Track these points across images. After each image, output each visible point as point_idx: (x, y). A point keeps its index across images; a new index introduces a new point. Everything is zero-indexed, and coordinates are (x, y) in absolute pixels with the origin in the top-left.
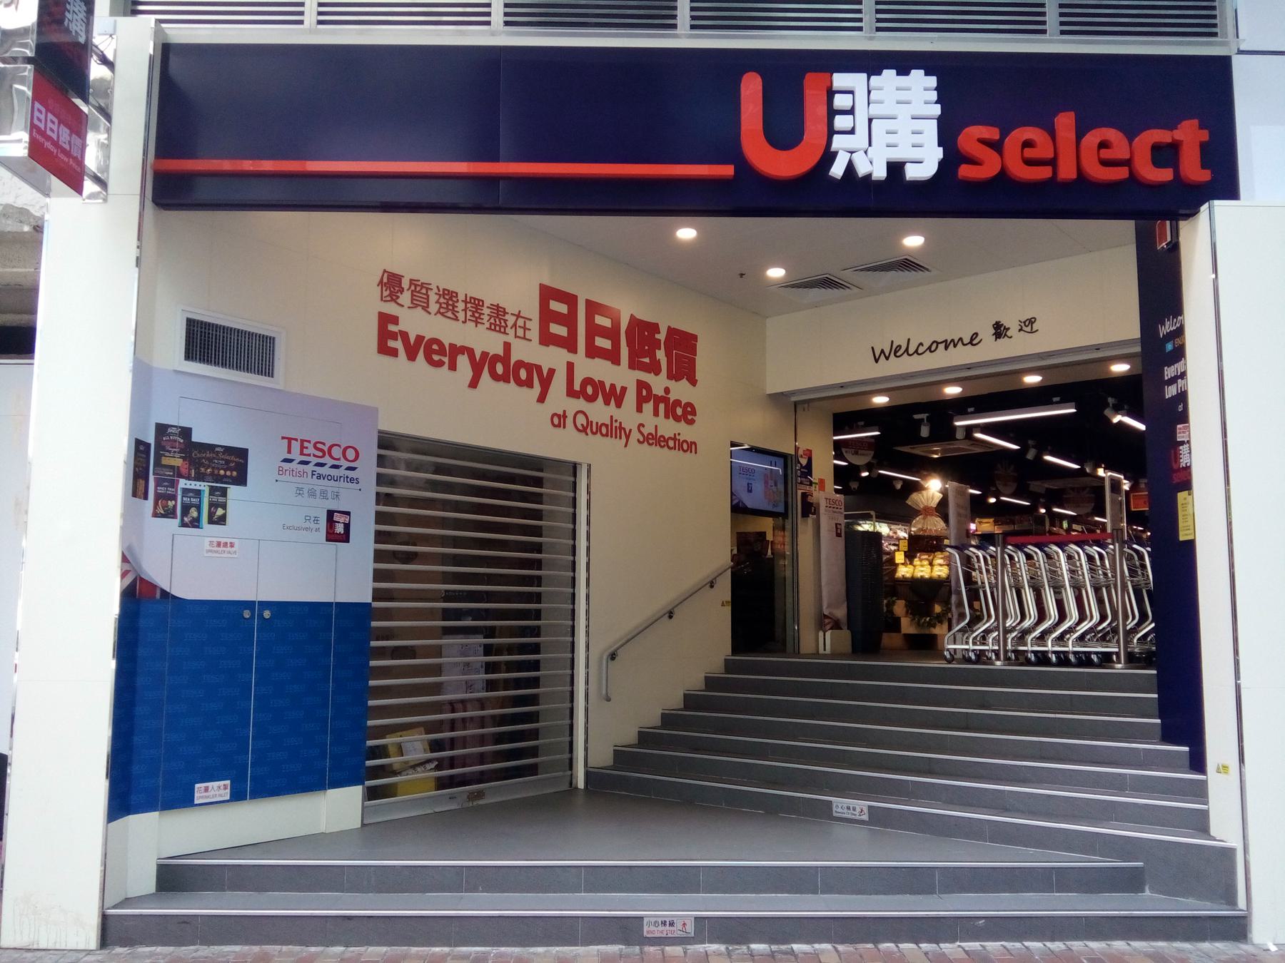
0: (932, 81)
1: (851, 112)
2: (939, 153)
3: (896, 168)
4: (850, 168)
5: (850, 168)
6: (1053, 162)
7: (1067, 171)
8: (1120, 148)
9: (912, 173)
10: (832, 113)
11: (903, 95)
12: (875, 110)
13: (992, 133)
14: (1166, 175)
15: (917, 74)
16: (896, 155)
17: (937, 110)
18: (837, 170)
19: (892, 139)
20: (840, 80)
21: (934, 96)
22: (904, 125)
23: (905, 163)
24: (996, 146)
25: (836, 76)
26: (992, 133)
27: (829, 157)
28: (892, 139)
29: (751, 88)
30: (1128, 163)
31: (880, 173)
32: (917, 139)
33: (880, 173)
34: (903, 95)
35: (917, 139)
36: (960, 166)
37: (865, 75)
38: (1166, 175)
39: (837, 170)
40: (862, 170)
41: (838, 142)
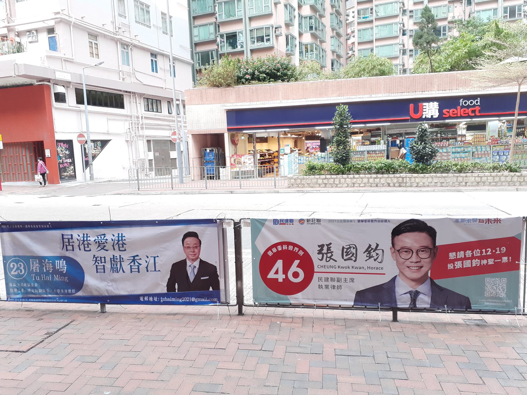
0: (438, 104)
1: (426, 108)
2: (438, 114)
3: (432, 116)
4: (426, 117)
5: (426, 117)
6: (457, 114)
8: (466, 112)
9: (434, 117)
10: (423, 109)
11: (433, 106)
12: (429, 108)
14: (473, 114)
16: (432, 114)
17: (438, 108)
18: (424, 117)
19: (432, 112)
20: (424, 104)
21: (438, 106)
22: (433, 110)
24: (448, 112)
27: (423, 115)
28: (432, 112)
29: (411, 106)
31: (430, 117)
32: (435, 112)
33: (430, 117)
34: (433, 106)
35: (435, 112)
37: (428, 103)
38: (473, 114)
39: (424, 117)
40: (427, 117)
41: (424, 113)
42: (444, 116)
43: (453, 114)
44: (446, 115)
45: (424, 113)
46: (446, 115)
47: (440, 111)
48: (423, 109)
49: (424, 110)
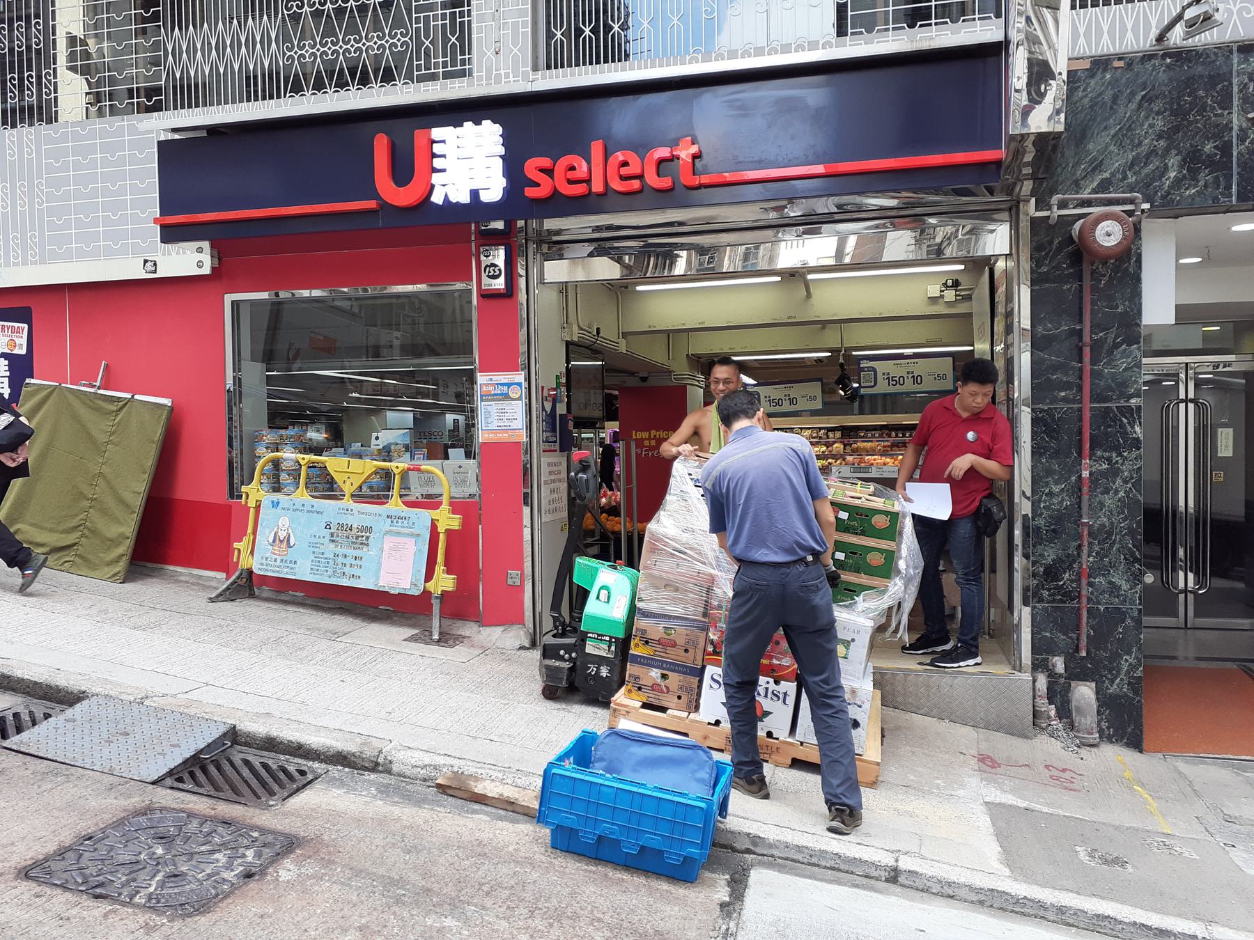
3: (475, 194)
6: (588, 181)
7: (597, 187)
9: (486, 197)
12: (461, 153)
13: (545, 162)
15: (487, 123)
18: (437, 198)
20: (437, 133)
23: (478, 190)
24: (549, 172)
25: (434, 130)
26: (545, 162)
30: (640, 177)
33: (465, 198)
36: (506, 191)
40: (453, 199)
41: (436, 179)
42: (530, 192)
43: (570, 182)
44: (538, 185)
45: (436, 179)
46: (538, 185)
47: (512, 165)
48: (434, 156)
49: (437, 163)
